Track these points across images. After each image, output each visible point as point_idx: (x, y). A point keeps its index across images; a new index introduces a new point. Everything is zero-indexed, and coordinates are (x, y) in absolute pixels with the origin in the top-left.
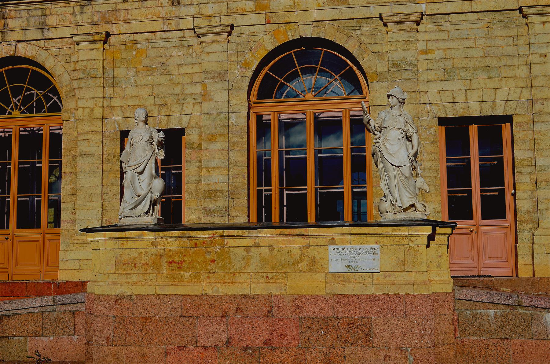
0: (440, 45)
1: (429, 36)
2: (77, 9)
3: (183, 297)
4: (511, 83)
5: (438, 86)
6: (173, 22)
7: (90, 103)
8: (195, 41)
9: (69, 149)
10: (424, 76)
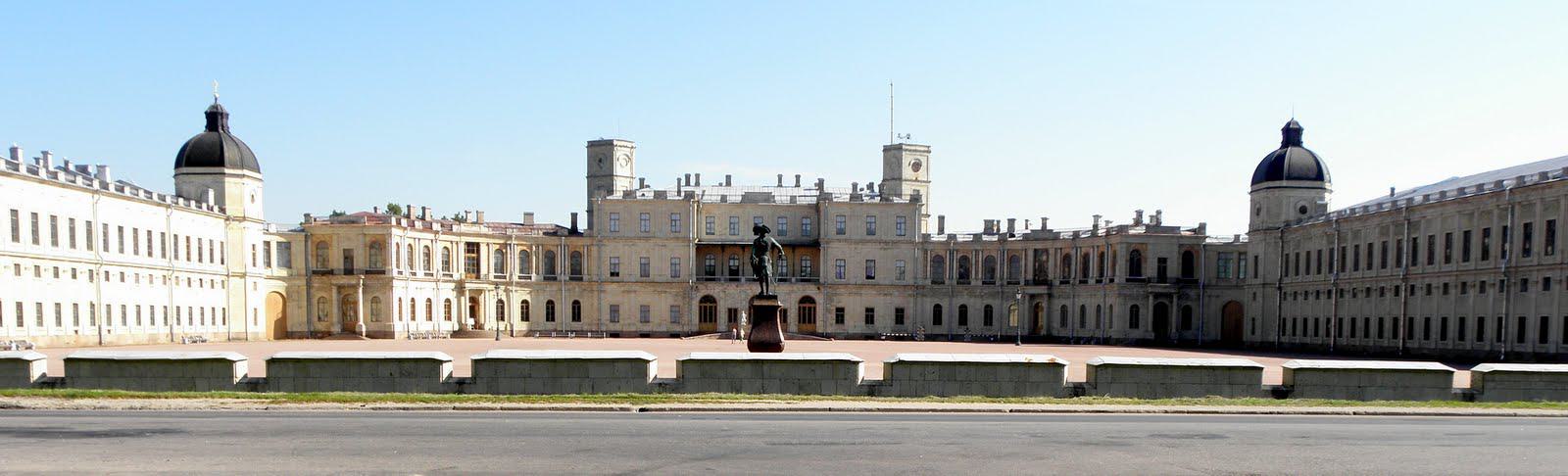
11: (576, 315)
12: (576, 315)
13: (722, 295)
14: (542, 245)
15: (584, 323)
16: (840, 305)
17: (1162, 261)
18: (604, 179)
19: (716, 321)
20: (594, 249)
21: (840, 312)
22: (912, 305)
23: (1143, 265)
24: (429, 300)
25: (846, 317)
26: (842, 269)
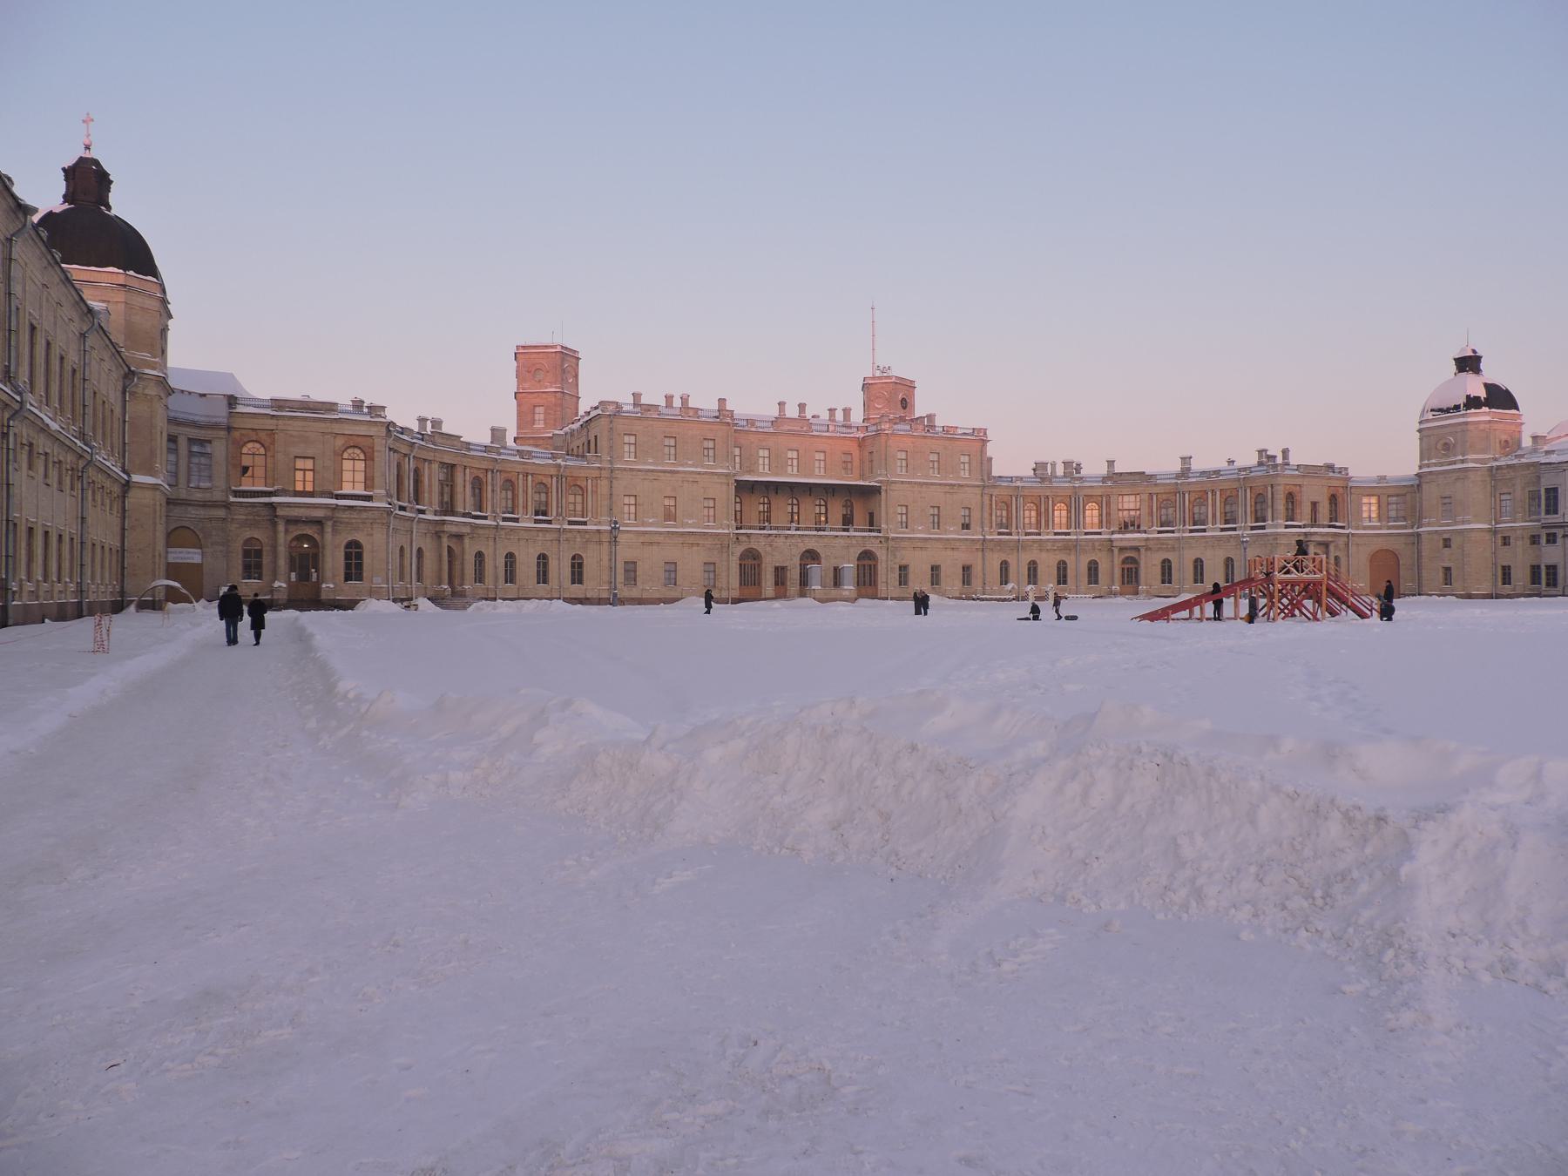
11: (577, 575)
12: (577, 575)
13: (768, 549)
14: (532, 474)
15: (590, 587)
16: (904, 562)
17: (1314, 504)
18: (544, 395)
19: (759, 584)
20: (604, 483)
21: (903, 569)
22: (980, 562)
23: (1299, 511)
24: (402, 549)
25: (911, 576)
26: (904, 517)
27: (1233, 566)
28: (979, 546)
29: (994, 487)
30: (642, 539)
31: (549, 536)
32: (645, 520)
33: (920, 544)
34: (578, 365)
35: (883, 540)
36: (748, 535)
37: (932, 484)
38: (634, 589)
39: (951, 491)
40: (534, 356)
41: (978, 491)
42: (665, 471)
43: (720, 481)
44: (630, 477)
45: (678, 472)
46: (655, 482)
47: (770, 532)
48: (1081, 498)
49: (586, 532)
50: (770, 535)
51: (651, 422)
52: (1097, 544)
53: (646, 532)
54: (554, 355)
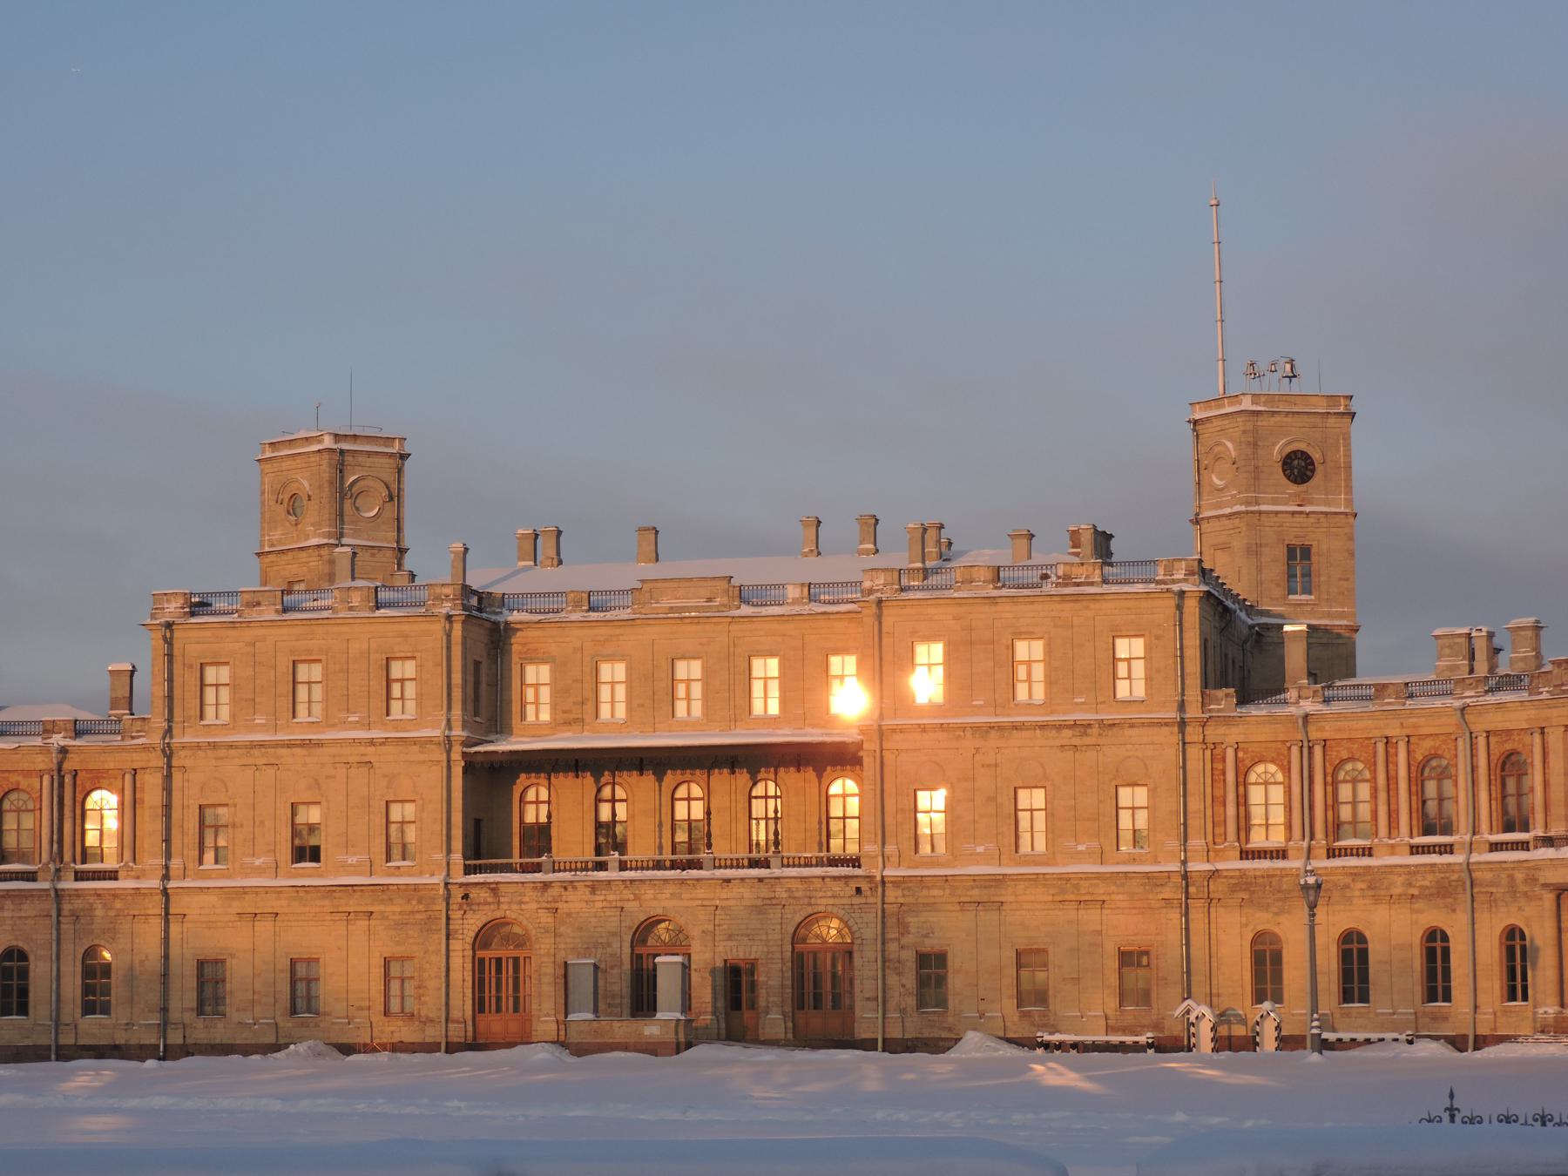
0: (729, 922)
1: (721, 917)
2: (539, 894)
3: (598, 1043)
4: (759, 943)
5: (723, 943)
6: (591, 903)
7: (548, 947)
8: (602, 914)
9: (536, 971)
10: (717, 939)
13: (546, 919)
16: (930, 945)
18: (303, 554)
25: (955, 982)
27: (1446, 952)
28: (1172, 892)
29: (1228, 721)
30: (237, 906)
31: (29, 909)
32: (247, 860)
33: (976, 894)
34: (400, 471)
35: (865, 886)
36: (494, 889)
37: (1015, 727)
38: (220, 1025)
39: (1076, 741)
40: (285, 465)
41: (1170, 736)
42: (290, 745)
43: (422, 757)
44: (213, 762)
45: (320, 744)
46: (271, 771)
47: (551, 877)
48: (1481, 741)
49: (115, 894)
50: (546, 885)
51: (261, 632)
52: (1519, 876)
53: (244, 891)
54: (316, 458)
